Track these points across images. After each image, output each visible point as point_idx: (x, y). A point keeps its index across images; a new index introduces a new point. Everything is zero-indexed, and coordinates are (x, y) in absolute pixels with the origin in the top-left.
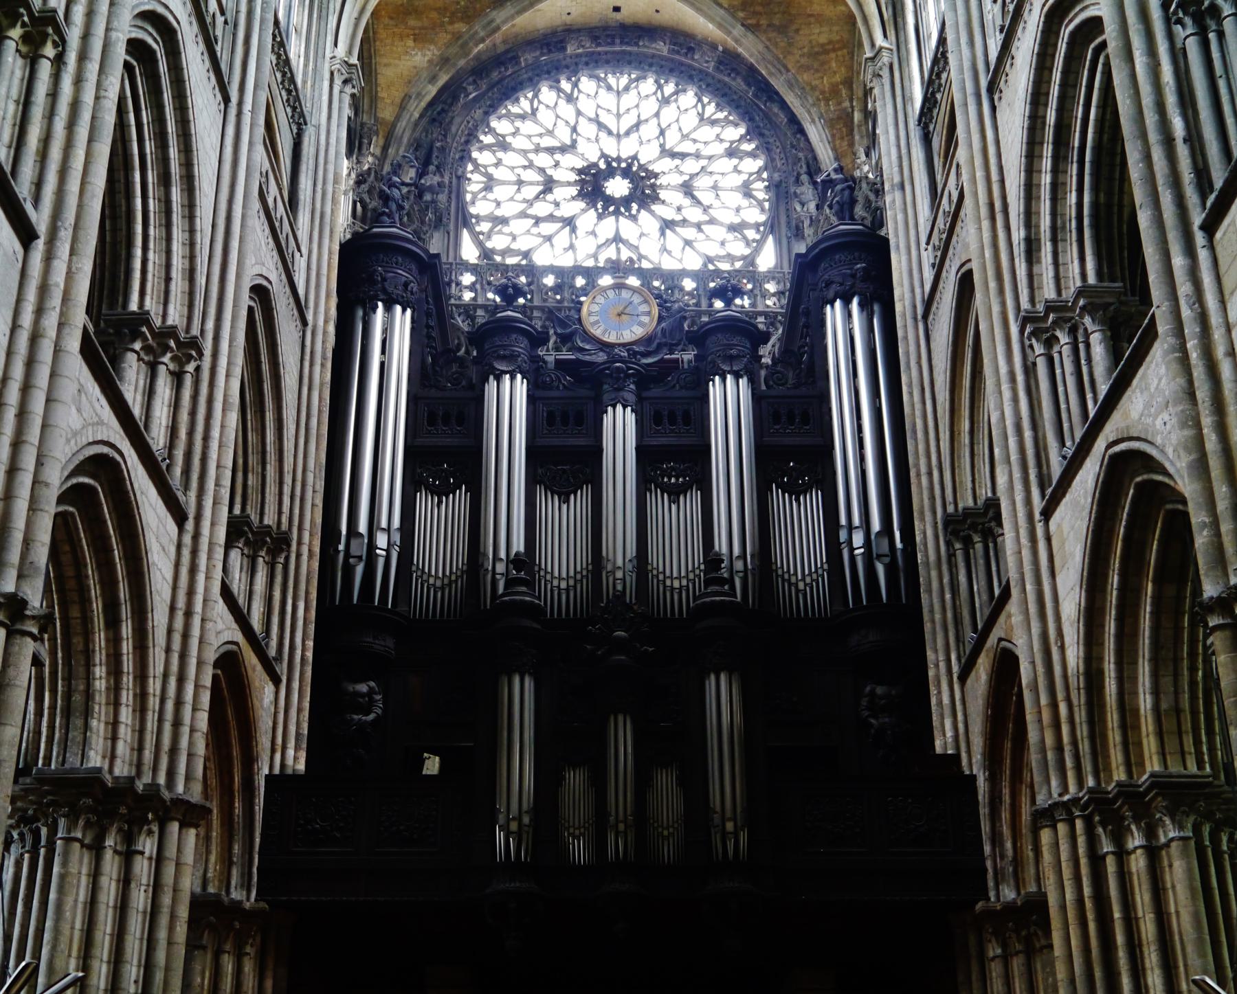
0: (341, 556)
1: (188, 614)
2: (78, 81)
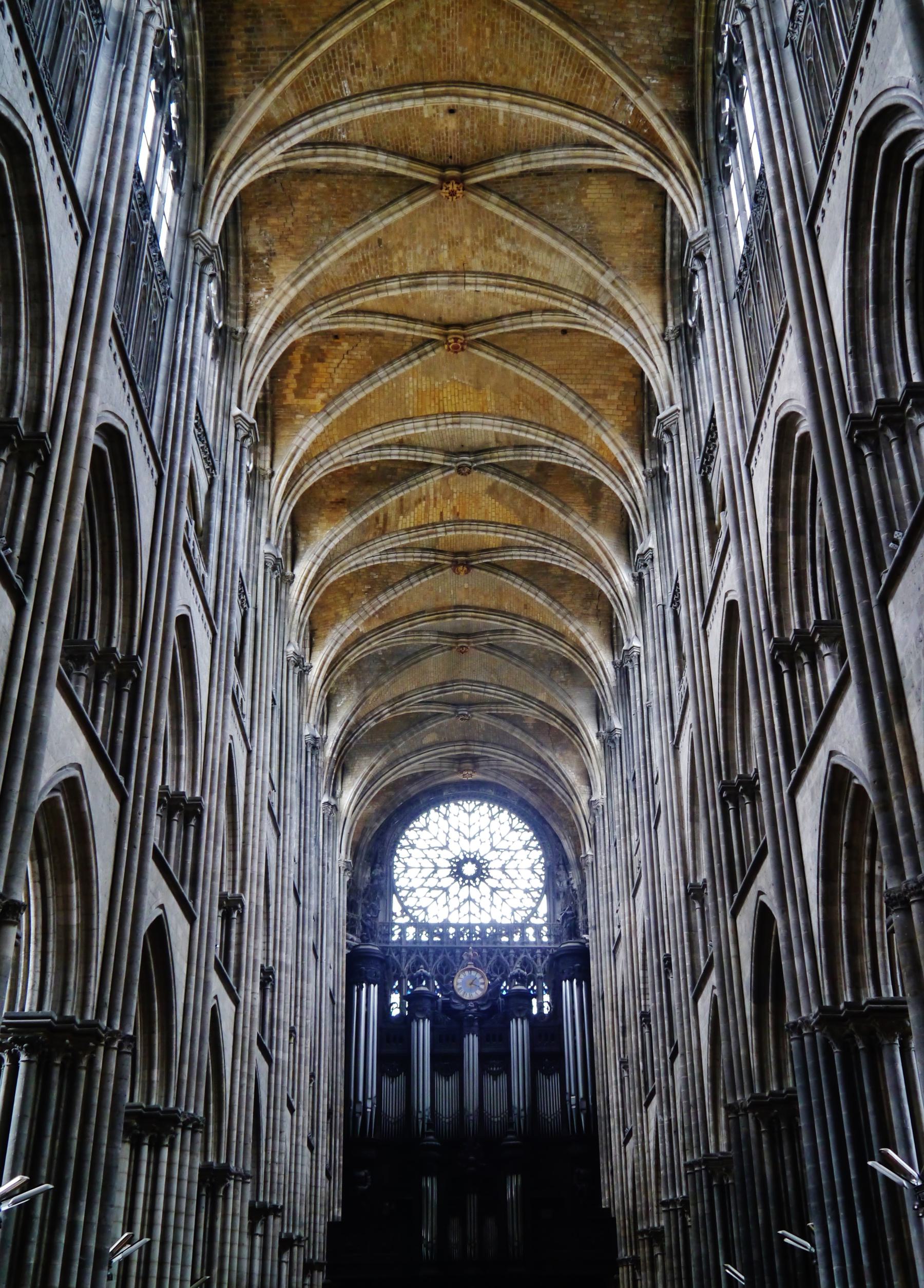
0: (351, 1113)
1: (316, 1187)
2: (300, 1045)
